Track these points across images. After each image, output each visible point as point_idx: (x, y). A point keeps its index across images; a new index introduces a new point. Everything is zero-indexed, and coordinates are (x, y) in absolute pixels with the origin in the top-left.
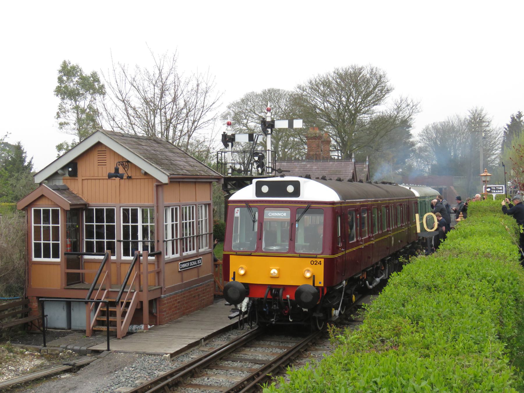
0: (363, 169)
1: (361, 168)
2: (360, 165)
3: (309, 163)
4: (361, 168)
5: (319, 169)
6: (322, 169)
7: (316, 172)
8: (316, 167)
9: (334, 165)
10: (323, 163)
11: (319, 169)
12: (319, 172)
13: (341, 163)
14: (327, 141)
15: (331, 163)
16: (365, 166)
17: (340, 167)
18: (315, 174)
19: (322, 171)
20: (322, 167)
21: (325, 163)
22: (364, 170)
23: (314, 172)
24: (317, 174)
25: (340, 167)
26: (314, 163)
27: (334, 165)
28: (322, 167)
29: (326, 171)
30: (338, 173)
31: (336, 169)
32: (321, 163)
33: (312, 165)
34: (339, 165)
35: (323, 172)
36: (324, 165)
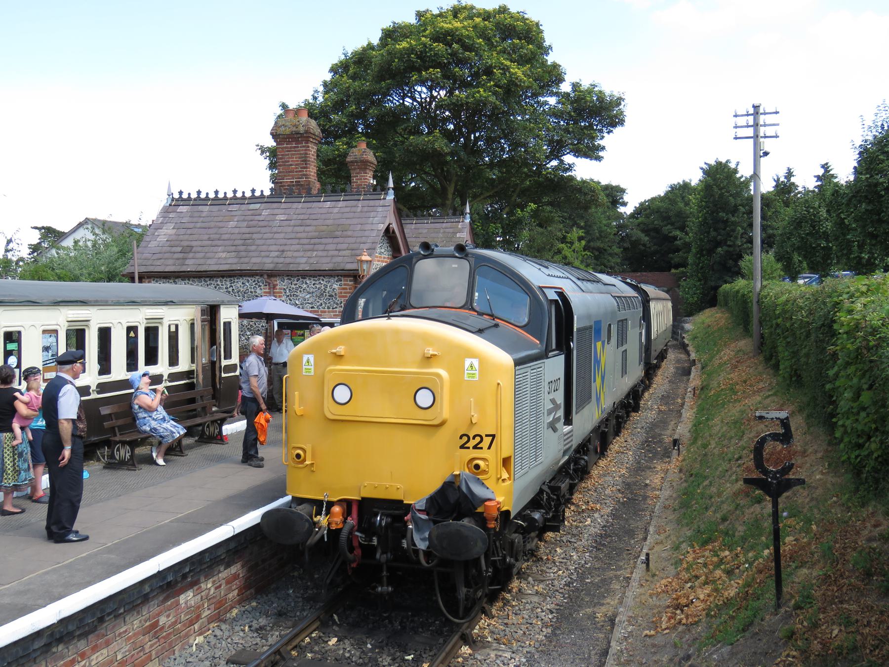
1: (451, 230)
2: (449, 225)
4: (451, 230)
5: (292, 223)
8: (282, 217)
9: (336, 210)
11: (292, 223)
12: (290, 229)
14: (362, 161)
16: (460, 226)
17: (351, 215)
18: (276, 236)
20: (302, 217)
21: (309, 205)
23: (275, 229)
24: (282, 235)
25: (351, 215)
26: (283, 206)
29: (307, 229)
30: (339, 233)
32: (300, 205)
33: (276, 211)
34: (348, 210)
36: (309, 211)
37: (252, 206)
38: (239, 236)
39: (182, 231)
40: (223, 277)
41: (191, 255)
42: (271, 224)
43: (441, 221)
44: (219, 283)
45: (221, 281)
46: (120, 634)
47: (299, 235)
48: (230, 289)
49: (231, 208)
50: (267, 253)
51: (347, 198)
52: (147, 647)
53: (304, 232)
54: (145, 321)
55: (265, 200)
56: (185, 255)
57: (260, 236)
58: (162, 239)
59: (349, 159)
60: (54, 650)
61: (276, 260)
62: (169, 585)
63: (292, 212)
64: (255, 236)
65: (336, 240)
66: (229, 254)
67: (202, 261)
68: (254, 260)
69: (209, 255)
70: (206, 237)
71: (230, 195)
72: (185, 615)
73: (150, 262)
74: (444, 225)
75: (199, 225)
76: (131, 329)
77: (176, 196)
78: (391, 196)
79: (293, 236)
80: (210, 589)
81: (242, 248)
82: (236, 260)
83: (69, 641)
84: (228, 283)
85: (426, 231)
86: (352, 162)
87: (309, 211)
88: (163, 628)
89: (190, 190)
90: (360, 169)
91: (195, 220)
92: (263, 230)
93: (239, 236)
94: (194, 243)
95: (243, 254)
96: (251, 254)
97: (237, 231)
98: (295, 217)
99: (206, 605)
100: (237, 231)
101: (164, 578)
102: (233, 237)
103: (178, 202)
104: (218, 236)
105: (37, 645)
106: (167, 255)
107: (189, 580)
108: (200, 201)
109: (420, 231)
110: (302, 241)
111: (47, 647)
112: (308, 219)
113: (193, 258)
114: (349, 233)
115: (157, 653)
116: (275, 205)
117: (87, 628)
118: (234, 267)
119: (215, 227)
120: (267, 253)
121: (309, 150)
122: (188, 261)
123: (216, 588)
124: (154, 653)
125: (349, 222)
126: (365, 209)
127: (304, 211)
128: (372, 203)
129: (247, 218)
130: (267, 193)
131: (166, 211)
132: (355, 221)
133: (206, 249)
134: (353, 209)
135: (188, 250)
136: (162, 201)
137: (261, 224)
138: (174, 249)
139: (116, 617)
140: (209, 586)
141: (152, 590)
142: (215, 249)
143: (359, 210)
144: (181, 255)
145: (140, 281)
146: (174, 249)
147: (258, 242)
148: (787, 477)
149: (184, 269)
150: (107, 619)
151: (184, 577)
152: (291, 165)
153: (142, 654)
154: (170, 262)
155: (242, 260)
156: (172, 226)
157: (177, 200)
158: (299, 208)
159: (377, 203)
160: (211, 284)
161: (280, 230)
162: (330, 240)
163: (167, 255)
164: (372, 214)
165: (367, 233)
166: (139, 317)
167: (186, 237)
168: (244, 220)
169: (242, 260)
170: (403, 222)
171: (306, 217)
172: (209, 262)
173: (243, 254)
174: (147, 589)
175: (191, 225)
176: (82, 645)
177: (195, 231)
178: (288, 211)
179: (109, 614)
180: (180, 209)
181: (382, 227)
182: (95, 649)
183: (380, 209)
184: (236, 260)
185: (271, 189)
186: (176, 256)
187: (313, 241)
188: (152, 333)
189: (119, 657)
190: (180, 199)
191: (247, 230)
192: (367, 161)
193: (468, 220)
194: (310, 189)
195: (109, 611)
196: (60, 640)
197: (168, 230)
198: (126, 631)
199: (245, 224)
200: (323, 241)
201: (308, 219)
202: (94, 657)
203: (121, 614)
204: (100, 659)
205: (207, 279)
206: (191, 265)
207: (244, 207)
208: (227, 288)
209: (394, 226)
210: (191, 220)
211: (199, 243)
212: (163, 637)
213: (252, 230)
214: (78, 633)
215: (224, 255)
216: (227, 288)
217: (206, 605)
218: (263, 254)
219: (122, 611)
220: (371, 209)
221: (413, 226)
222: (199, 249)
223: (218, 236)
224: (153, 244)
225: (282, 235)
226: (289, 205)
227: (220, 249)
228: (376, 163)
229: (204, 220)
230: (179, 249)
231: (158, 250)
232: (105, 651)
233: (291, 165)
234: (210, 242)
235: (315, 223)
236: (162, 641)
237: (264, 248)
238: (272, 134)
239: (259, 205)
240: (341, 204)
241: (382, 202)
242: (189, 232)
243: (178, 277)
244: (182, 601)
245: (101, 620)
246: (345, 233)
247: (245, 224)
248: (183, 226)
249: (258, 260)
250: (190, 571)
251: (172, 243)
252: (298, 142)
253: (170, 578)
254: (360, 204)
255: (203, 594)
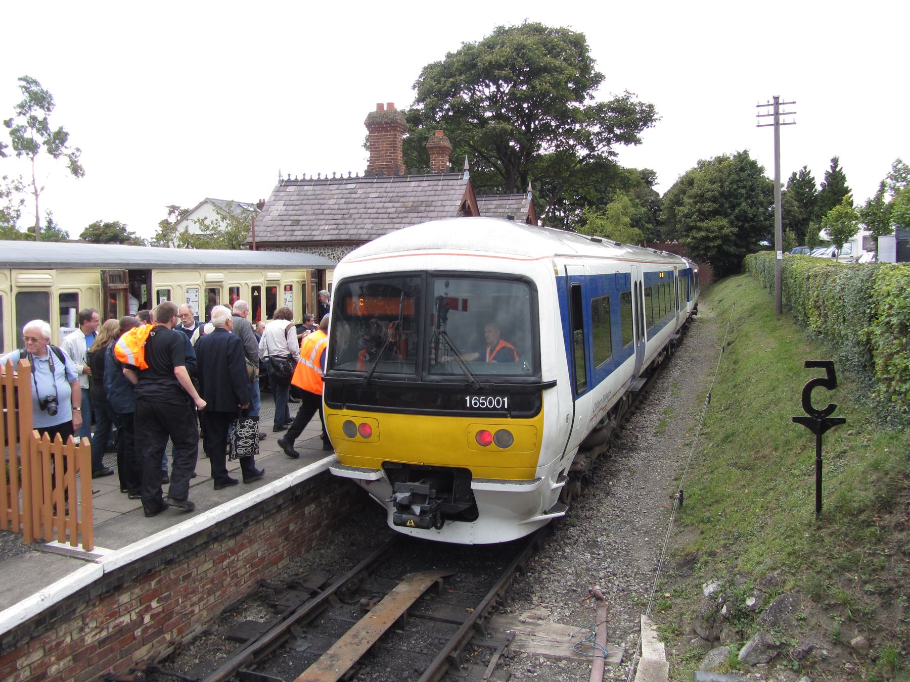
0: (519, 209)
1: (516, 206)
2: (513, 201)
3: (363, 185)
5: (383, 200)
6: (388, 199)
7: (372, 205)
9: (420, 189)
10: (394, 185)
11: (383, 200)
12: (381, 205)
13: (436, 182)
14: (439, 147)
15: (413, 184)
16: (524, 202)
17: (433, 193)
18: (370, 211)
19: (387, 205)
20: (391, 194)
21: (398, 184)
22: (522, 210)
23: (368, 205)
24: (375, 210)
25: (433, 193)
26: (375, 185)
27: (420, 189)
28: (391, 194)
29: (396, 205)
30: (422, 209)
31: (421, 199)
32: (389, 185)
33: (369, 190)
34: (430, 188)
35: (390, 205)
36: (397, 189)
37: (349, 186)
38: (339, 212)
39: (291, 207)
40: (325, 246)
41: (299, 228)
42: (365, 200)
43: (507, 198)
44: (322, 251)
45: (324, 249)
46: (260, 536)
47: (389, 210)
48: (332, 256)
49: (331, 187)
50: (363, 226)
51: (429, 178)
52: (280, 547)
53: (393, 207)
54: (266, 282)
55: (360, 181)
56: (295, 228)
57: (355, 211)
58: (276, 214)
59: (429, 144)
60: (211, 547)
61: (370, 231)
62: (298, 499)
63: (383, 190)
64: (352, 211)
65: (420, 215)
66: (330, 227)
67: (309, 233)
68: (351, 232)
69: (313, 227)
70: (311, 212)
71: (330, 177)
72: (309, 523)
73: (265, 234)
74: (509, 202)
75: (305, 202)
76: (256, 289)
77: (286, 178)
78: (467, 176)
79: (383, 211)
80: (328, 503)
81: (342, 221)
82: (336, 232)
83: (222, 541)
84: (330, 251)
85: (494, 206)
86: (432, 148)
87: (397, 189)
88: (292, 532)
89: (297, 174)
90: (438, 154)
91: (301, 197)
92: (359, 206)
93: (339, 212)
94: (301, 218)
95: (343, 226)
96: (349, 226)
97: (336, 207)
98: (385, 194)
99: (325, 516)
100: (336, 207)
101: (294, 493)
102: (333, 212)
103: (286, 184)
104: (321, 212)
105: (199, 542)
106: (278, 228)
107: (312, 495)
108: (304, 182)
109: (489, 206)
110: (391, 215)
111: (207, 544)
112: (397, 196)
113: (300, 230)
114: (432, 208)
115: (288, 553)
116: (369, 185)
117: (236, 531)
118: (334, 238)
119: (318, 204)
120: (362, 226)
121: (396, 138)
122: (296, 233)
123: (332, 503)
124: (285, 552)
125: (431, 198)
126: (445, 187)
127: (393, 189)
128: (451, 182)
129: (345, 196)
130: (362, 174)
131: (277, 191)
132: (436, 198)
133: (311, 223)
134: (435, 188)
135: (297, 222)
136: (275, 183)
137: (356, 201)
138: (284, 223)
139: (257, 522)
140: (327, 500)
141: (284, 503)
142: (320, 222)
143: (440, 188)
144: (290, 228)
145: (258, 249)
146: (284, 223)
147: (354, 216)
148: (829, 417)
149: (293, 239)
150: (251, 523)
151: (309, 492)
152: (382, 150)
153: (276, 552)
154: (282, 233)
155: (342, 232)
156: (282, 203)
157: (286, 181)
158: (390, 187)
159: (455, 182)
160: (315, 252)
161: (372, 205)
162: (416, 215)
163: (278, 228)
164: (452, 192)
165: (447, 209)
166: (261, 279)
167: (294, 212)
168: (342, 198)
169: (342, 232)
170: (477, 199)
171: (395, 194)
172: (314, 233)
173: (343, 226)
174: (280, 501)
175: (299, 202)
176: (231, 543)
177: (301, 207)
178: (379, 190)
179: (252, 520)
180: (291, 189)
181: (459, 203)
182: (242, 547)
183: (458, 188)
184: (336, 232)
185: (366, 172)
186: (286, 228)
187: (401, 215)
188: (271, 293)
189: (259, 555)
190: (289, 181)
191: (345, 206)
192: (445, 147)
193: (530, 197)
194: (398, 171)
195: (252, 517)
196: (215, 540)
197: (279, 208)
198: (264, 534)
199: (343, 201)
200: (410, 215)
201: (397, 196)
202: (241, 553)
203: (261, 520)
204: (245, 555)
205: (312, 248)
206: (299, 236)
207: (342, 187)
208: (329, 255)
209: (469, 202)
210: (297, 197)
211: (305, 217)
212: (293, 540)
213: (349, 206)
214: (229, 534)
215: (326, 228)
216: (329, 255)
217: (325, 516)
218: (359, 226)
219: (261, 518)
220: (450, 187)
221: (483, 202)
222: (306, 222)
223: (321, 212)
224: (268, 218)
225: (375, 210)
226: (381, 185)
227: (323, 222)
228: (451, 148)
229: (310, 197)
230: (289, 223)
231: (271, 223)
232: (248, 549)
233: (382, 150)
234: (314, 217)
235: (402, 200)
236: (292, 543)
237: (360, 221)
238: (365, 124)
239: (353, 186)
240: (425, 184)
241: (459, 182)
242: (297, 208)
243: (288, 246)
244: (306, 512)
245: (246, 524)
246: (428, 209)
247: (343, 201)
248: (291, 202)
249: (354, 231)
250: (314, 488)
251: (283, 218)
252: (387, 131)
253: (298, 493)
254: (440, 183)
255: (323, 506)
